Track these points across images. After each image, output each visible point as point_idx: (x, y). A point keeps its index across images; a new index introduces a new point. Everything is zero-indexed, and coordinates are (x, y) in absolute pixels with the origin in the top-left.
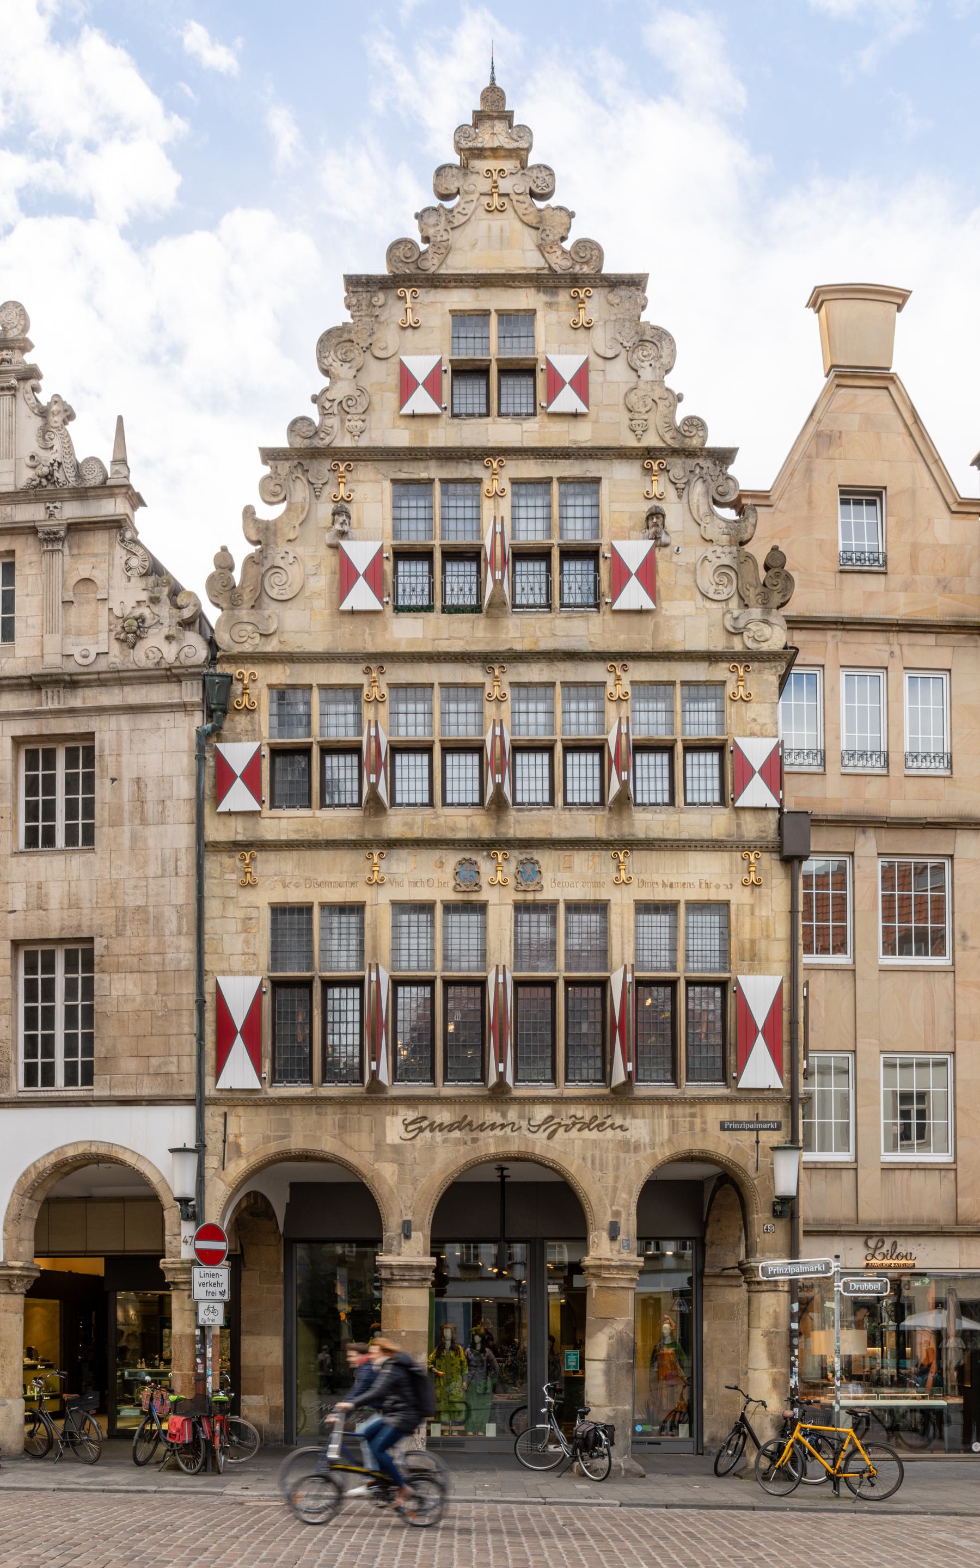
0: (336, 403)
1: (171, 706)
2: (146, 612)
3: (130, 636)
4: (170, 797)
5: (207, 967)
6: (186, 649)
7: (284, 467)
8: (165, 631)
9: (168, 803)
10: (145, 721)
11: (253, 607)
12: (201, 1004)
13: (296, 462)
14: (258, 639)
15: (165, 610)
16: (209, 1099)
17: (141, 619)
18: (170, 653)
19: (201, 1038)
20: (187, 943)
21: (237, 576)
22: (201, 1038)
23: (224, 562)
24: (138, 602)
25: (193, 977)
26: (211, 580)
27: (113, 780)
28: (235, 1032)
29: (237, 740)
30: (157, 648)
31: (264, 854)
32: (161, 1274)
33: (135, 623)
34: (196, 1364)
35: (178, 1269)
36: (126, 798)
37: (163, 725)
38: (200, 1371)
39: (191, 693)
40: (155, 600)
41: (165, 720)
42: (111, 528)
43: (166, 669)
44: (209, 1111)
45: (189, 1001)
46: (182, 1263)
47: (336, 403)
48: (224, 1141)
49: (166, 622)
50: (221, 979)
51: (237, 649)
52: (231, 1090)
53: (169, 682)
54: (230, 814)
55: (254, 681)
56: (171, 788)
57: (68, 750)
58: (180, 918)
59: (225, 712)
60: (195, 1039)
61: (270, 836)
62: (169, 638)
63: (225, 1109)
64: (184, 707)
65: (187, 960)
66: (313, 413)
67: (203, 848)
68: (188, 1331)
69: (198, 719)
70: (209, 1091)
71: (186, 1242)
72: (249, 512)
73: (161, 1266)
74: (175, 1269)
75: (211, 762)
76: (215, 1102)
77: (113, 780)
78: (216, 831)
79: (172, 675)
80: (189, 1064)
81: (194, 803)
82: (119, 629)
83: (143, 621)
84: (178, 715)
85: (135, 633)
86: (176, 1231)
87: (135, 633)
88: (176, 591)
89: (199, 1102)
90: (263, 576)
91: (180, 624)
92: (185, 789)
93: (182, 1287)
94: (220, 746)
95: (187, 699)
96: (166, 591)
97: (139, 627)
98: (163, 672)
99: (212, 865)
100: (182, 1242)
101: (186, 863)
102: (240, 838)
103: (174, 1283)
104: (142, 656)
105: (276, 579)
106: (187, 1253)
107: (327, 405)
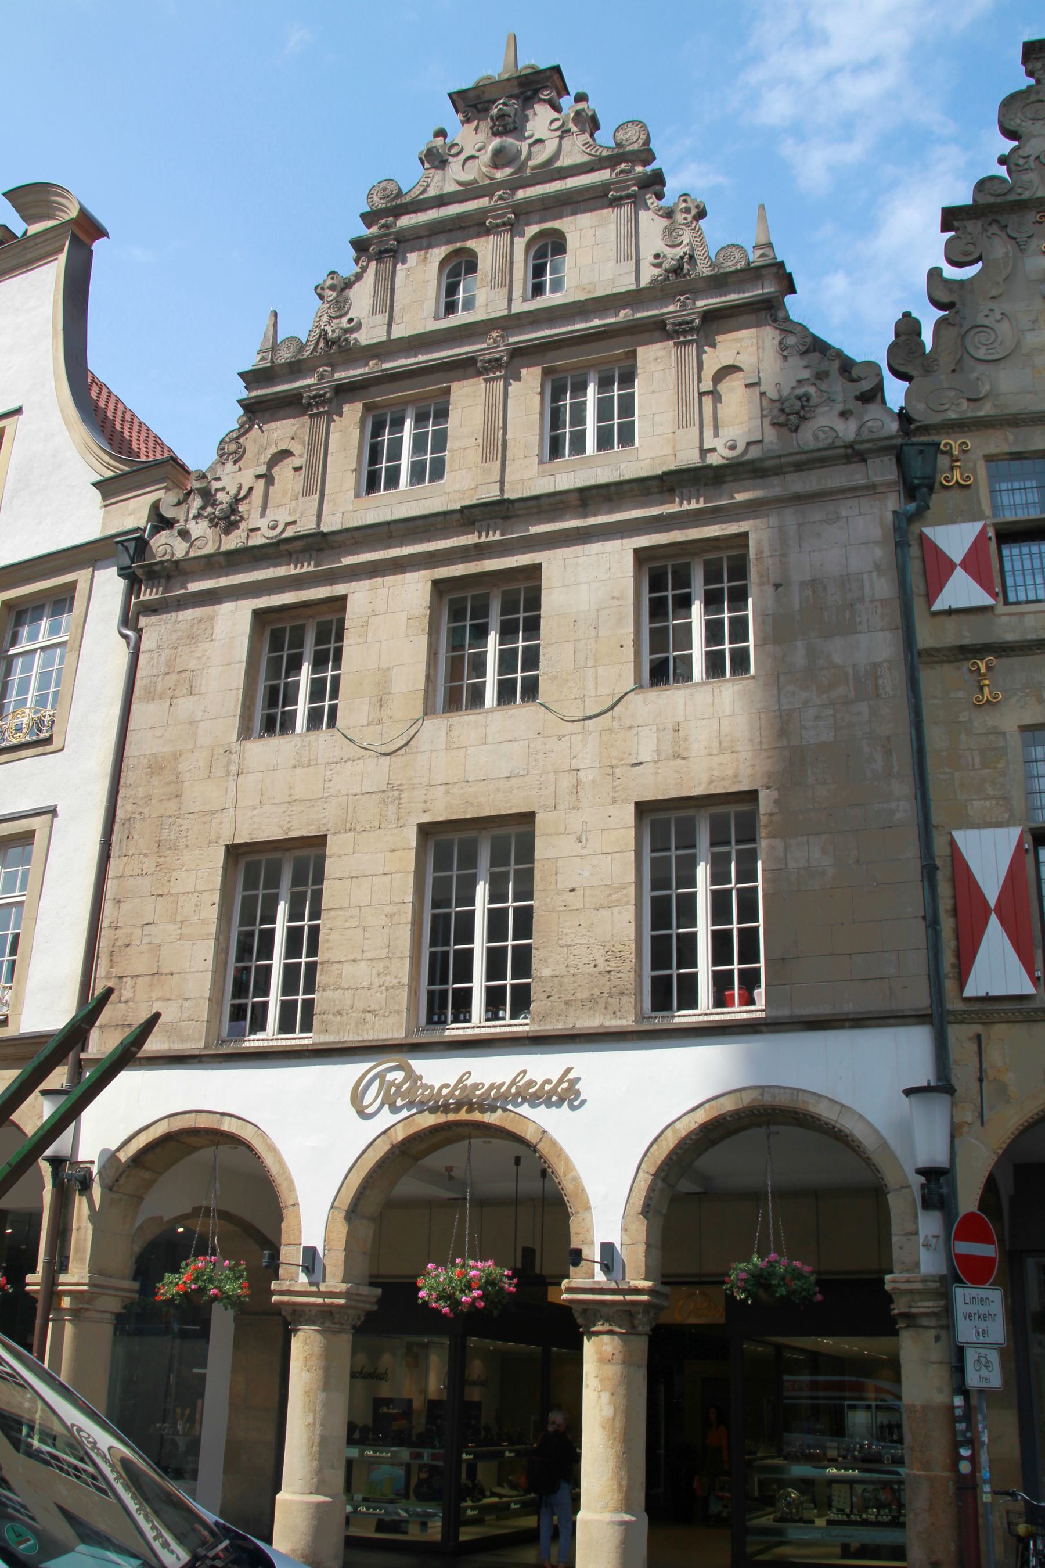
0: (1032, 158)
1: (855, 489)
2: (812, 390)
3: (791, 417)
4: (861, 600)
5: (935, 820)
6: (870, 424)
7: (973, 227)
8: (840, 407)
9: (859, 606)
10: (816, 513)
11: (954, 371)
12: (929, 871)
13: (989, 219)
14: (965, 404)
15: (837, 386)
16: (953, 1013)
17: (807, 397)
18: (847, 430)
19: (933, 923)
20: (903, 789)
21: (927, 337)
22: (933, 923)
23: (908, 327)
24: (799, 382)
25: (912, 835)
26: (892, 350)
27: (777, 586)
28: (995, 910)
29: (951, 520)
30: (829, 425)
31: (1004, 660)
32: (888, 1299)
33: (798, 404)
34: (959, 1457)
35: (918, 1292)
36: (797, 606)
37: (844, 514)
38: (965, 1467)
39: (884, 471)
40: (821, 376)
41: (846, 508)
42: (759, 310)
43: (845, 447)
44: (955, 1033)
45: (914, 869)
46: (924, 1281)
47: (1032, 158)
48: (981, 1080)
49: (840, 398)
50: (959, 836)
51: (936, 419)
52: (988, 999)
53: (849, 463)
54: (950, 612)
55: (965, 452)
56: (862, 588)
57: (707, 564)
58: (888, 753)
59: (931, 489)
60: (921, 925)
61: (1010, 637)
62: (844, 414)
63: (978, 1028)
64: (871, 489)
65: (904, 809)
66: (1002, 171)
67: (915, 658)
68: (940, 1398)
69: (892, 503)
70: (954, 1005)
71: (927, 1245)
72: (935, 274)
73: (888, 1287)
74: (911, 1292)
75: (915, 551)
76: (963, 1019)
77: (777, 586)
78: (926, 637)
79: (855, 454)
80: (917, 962)
81: (897, 604)
82: (775, 412)
83: (808, 400)
84: (864, 501)
85: (798, 413)
86: (910, 1228)
87: (798, 413)
88: (847, 366)
89: (936, 1018)
90: (963, 337)
91: (857, 398)
92: (883, 587)
93: (925, 1322)
94: (928, 531)
95: (877, 479)
96: (836, 365)
97: (803, 407)
98: (841, 451)
99: (931, 679)
100: (920, 1249)
101: (893, 682)
102: (966, 641)
103: (907, 1316)
104: (809, 436)
105: (982, 338)
106: (930, 1263)
107: (1021, 162)
